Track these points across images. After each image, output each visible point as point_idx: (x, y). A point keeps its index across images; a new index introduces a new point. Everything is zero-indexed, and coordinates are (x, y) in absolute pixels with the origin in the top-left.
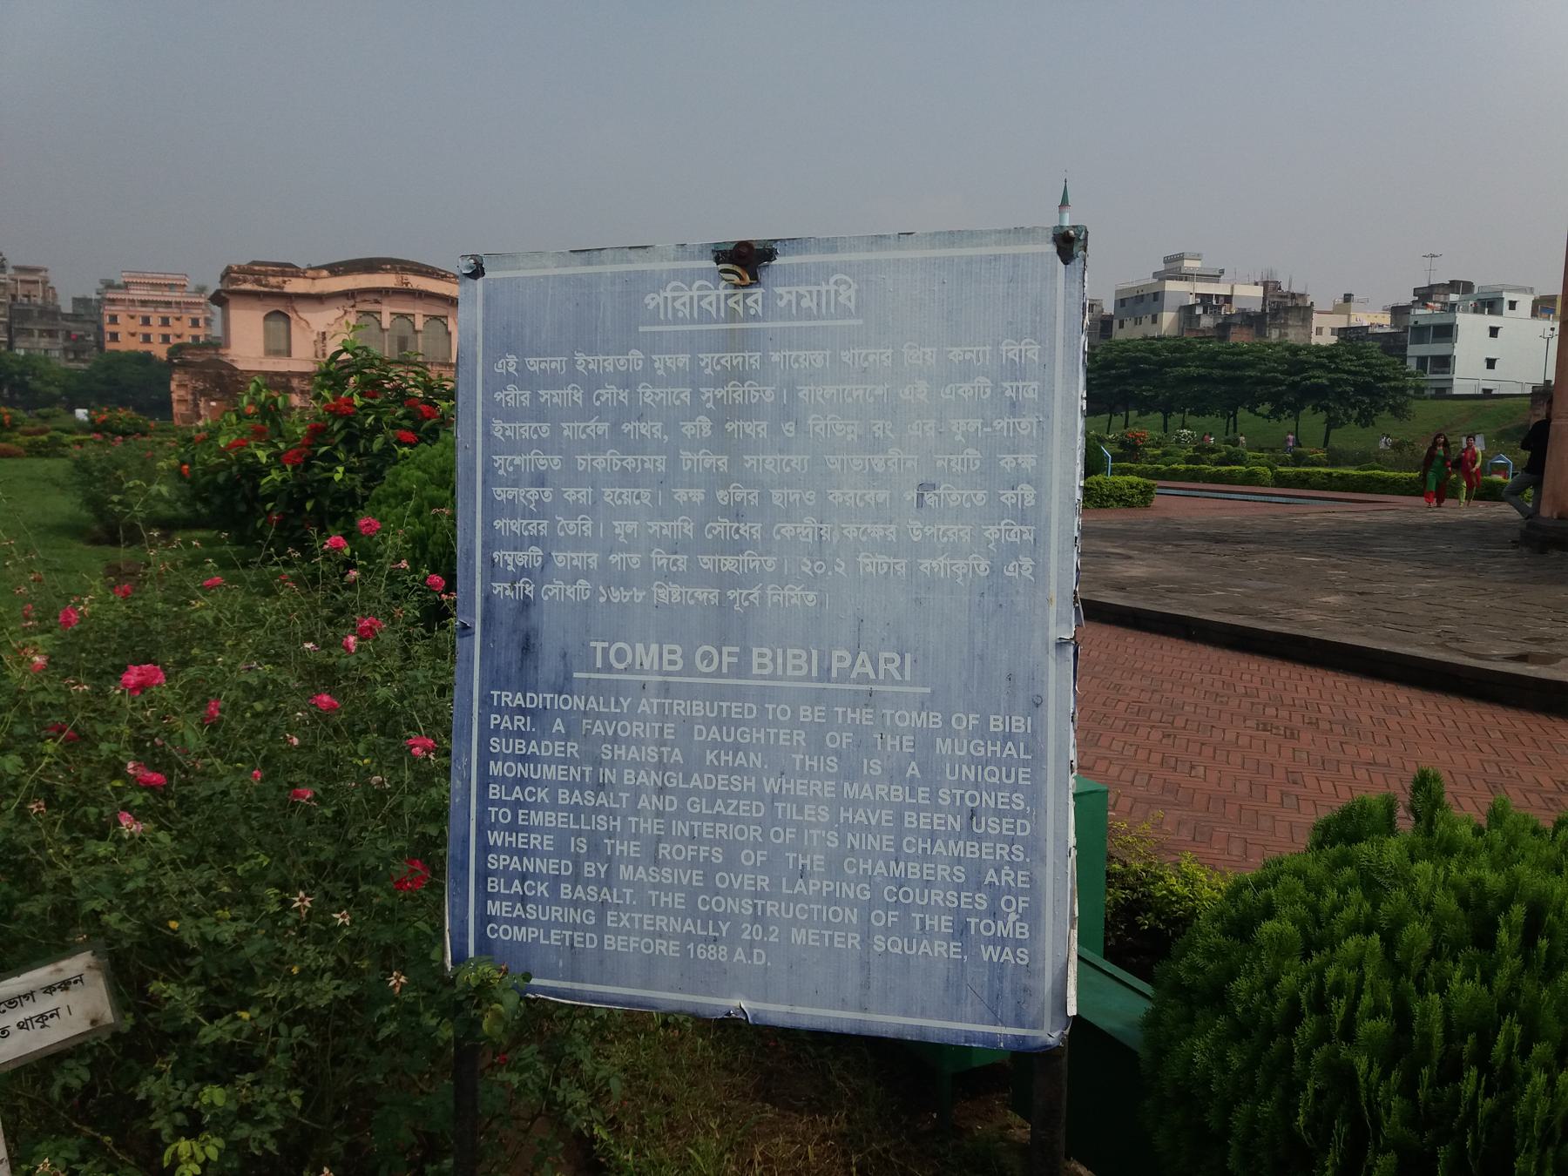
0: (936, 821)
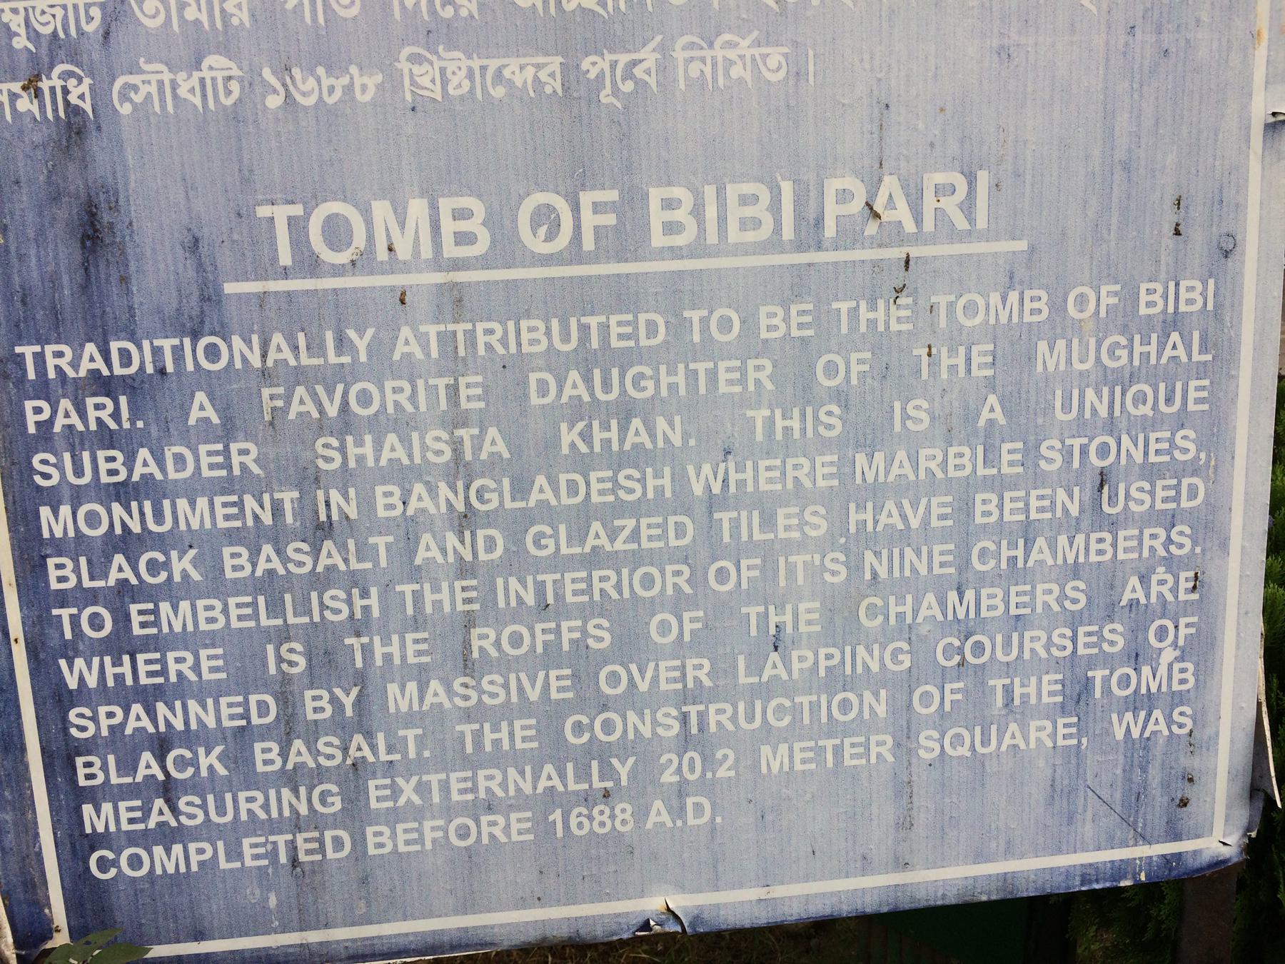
0: (1034, 503)
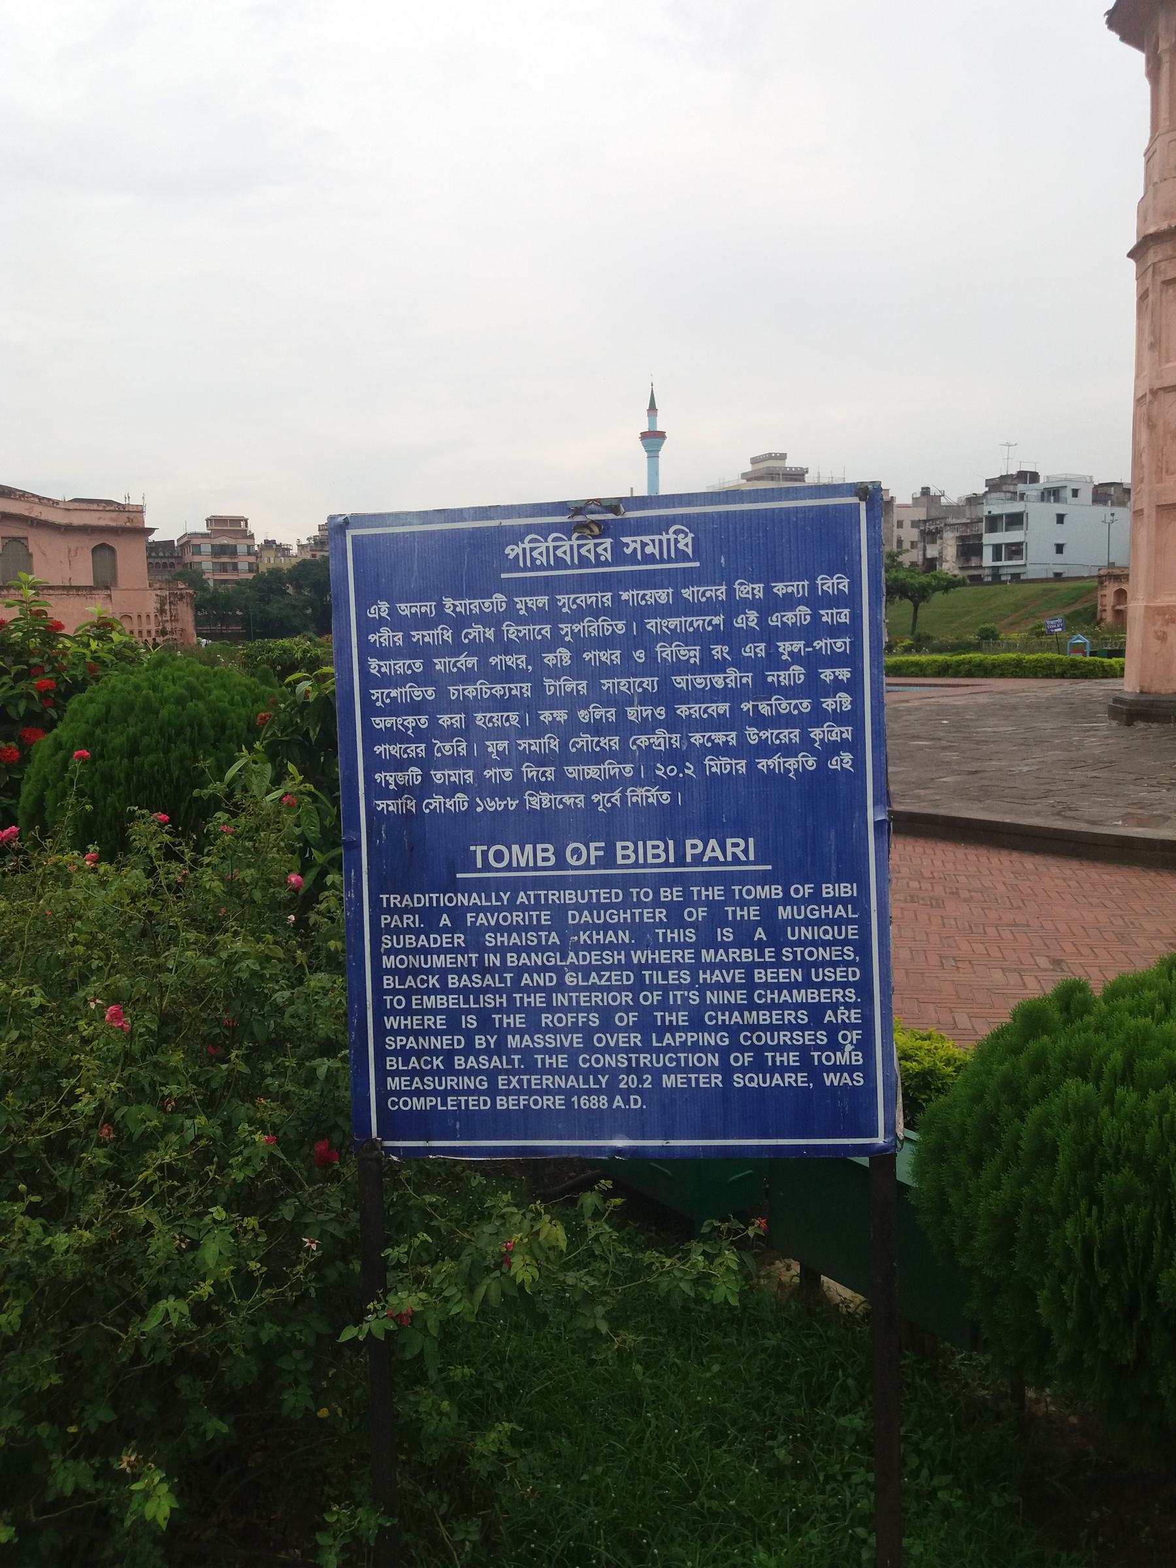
0: (781, 975)
